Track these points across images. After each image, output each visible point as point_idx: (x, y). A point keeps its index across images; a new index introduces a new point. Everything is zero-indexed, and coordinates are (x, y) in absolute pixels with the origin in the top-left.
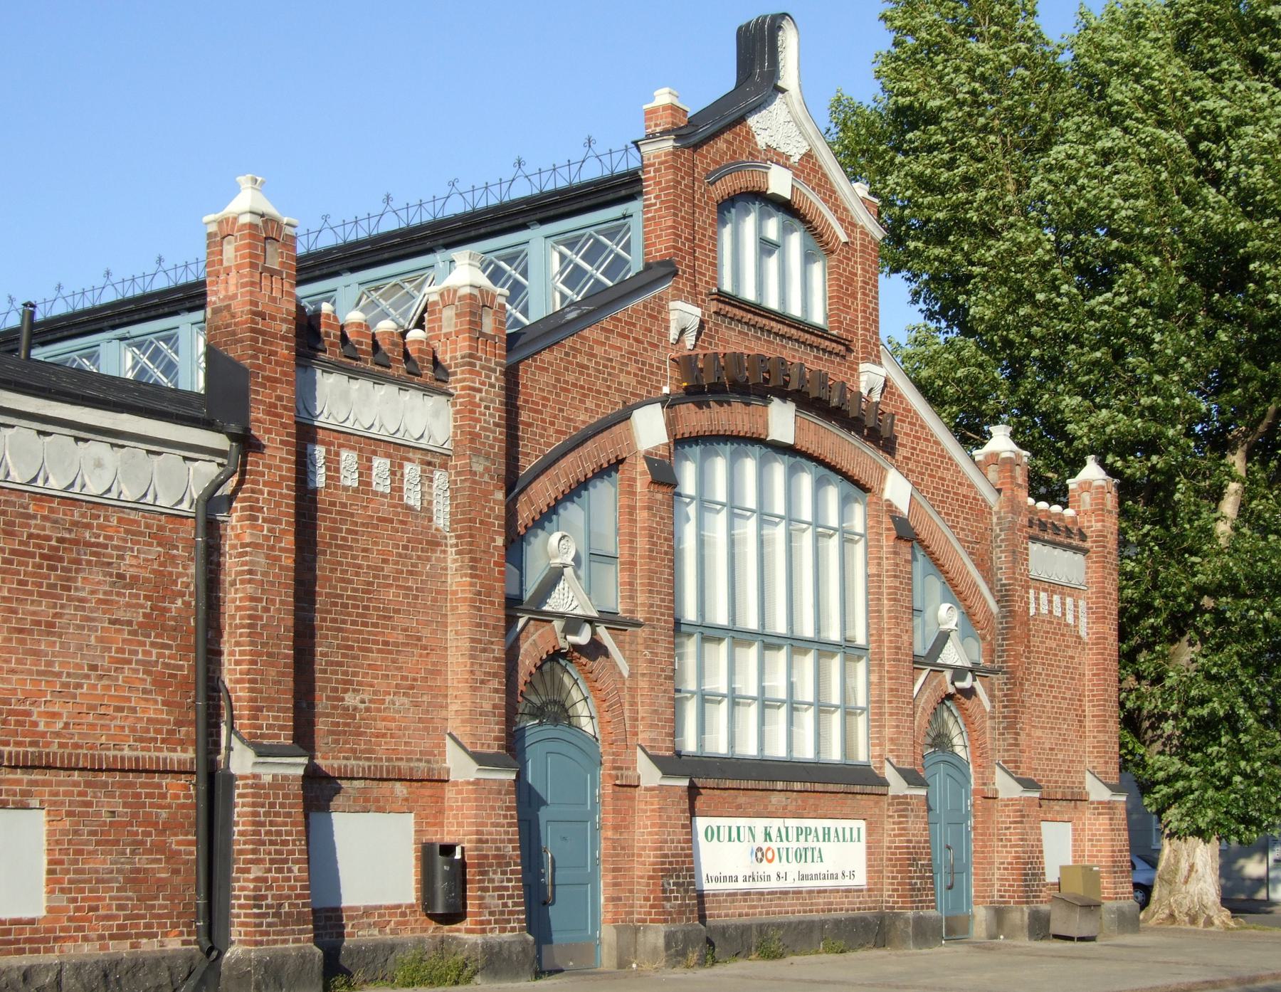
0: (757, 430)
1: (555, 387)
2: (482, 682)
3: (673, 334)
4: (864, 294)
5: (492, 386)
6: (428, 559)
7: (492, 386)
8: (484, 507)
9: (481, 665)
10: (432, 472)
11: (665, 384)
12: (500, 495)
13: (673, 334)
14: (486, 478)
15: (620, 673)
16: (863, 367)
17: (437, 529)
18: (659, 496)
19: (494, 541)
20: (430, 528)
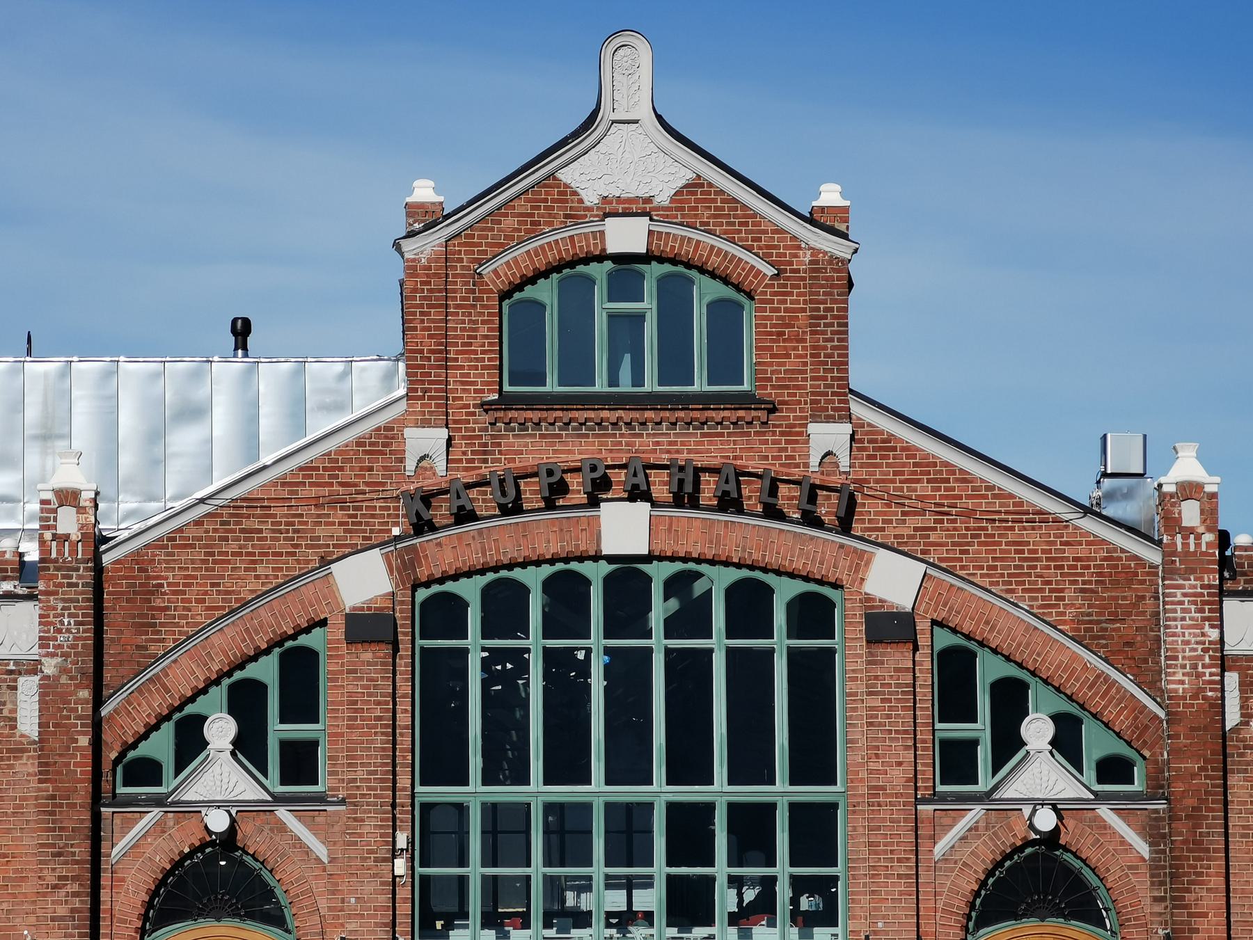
0: (585, 546)
1: (205, 562)
2: (55, 887)
3: (410, 465)
4: (813, 333)
5: (70, 585)
6: (10, 767)
7: (70, 585)
8: (61, 710)
9: (54, 870)
10: (16, 680)
11: (396, 524)
12: (85, 694)
13: (410, 465)
14: (64, 680)
15: (318, 860)
16: (813, 428)
17: (22, 736)
18: (367, 656)
19: (76, 741)
20: (13, 735)
